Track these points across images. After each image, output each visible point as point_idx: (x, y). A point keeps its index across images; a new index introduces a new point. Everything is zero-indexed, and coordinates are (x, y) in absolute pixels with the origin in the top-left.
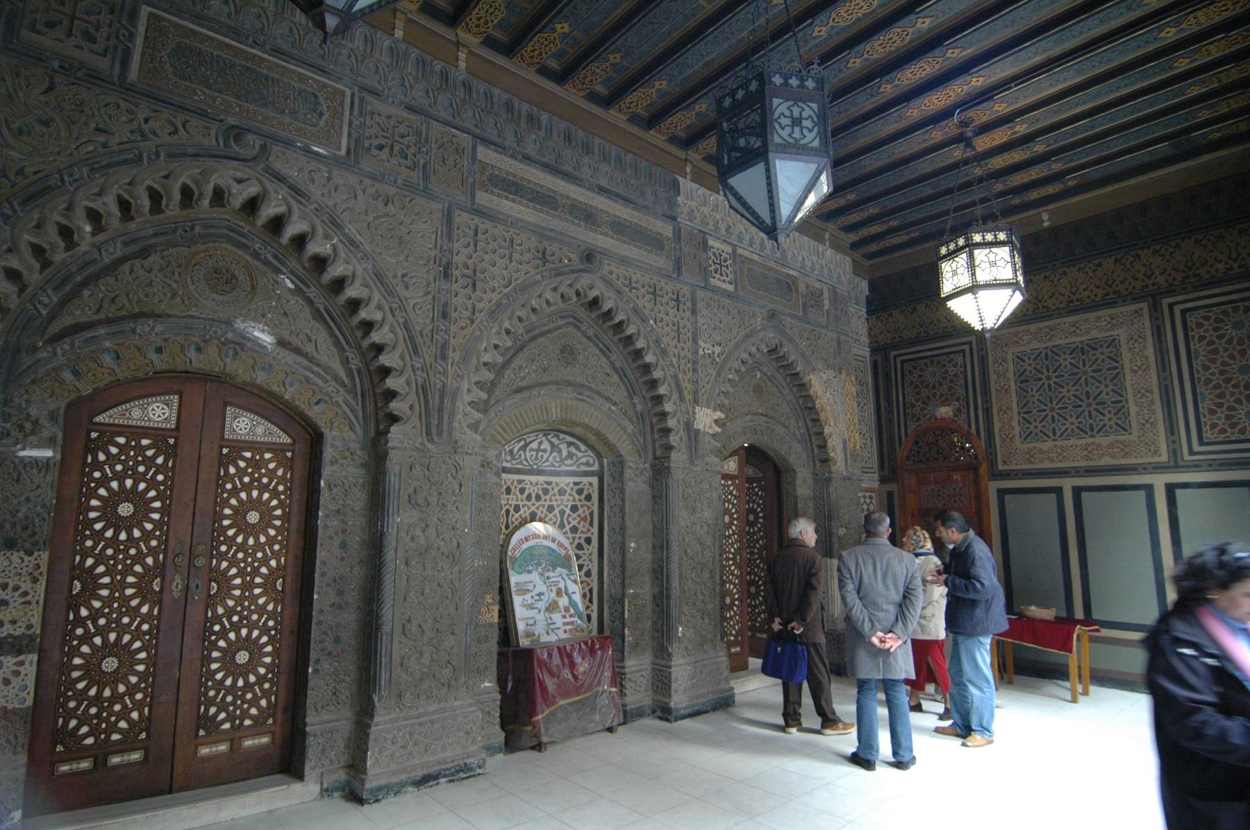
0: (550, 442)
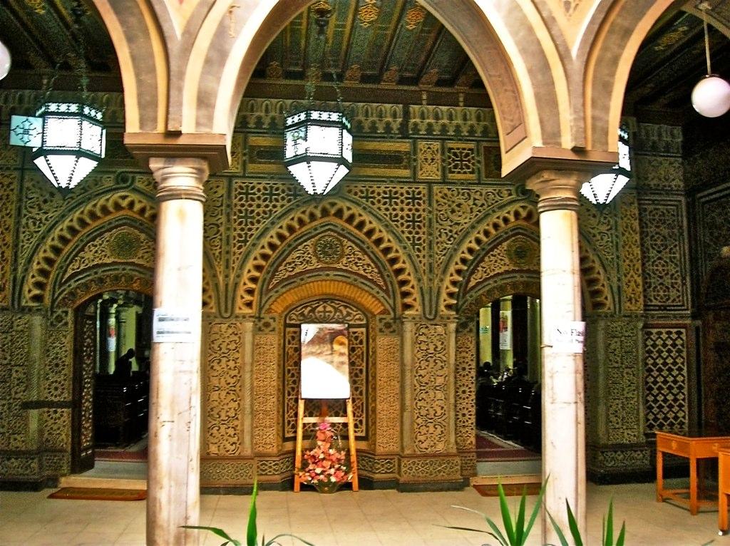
0: (332, 306)
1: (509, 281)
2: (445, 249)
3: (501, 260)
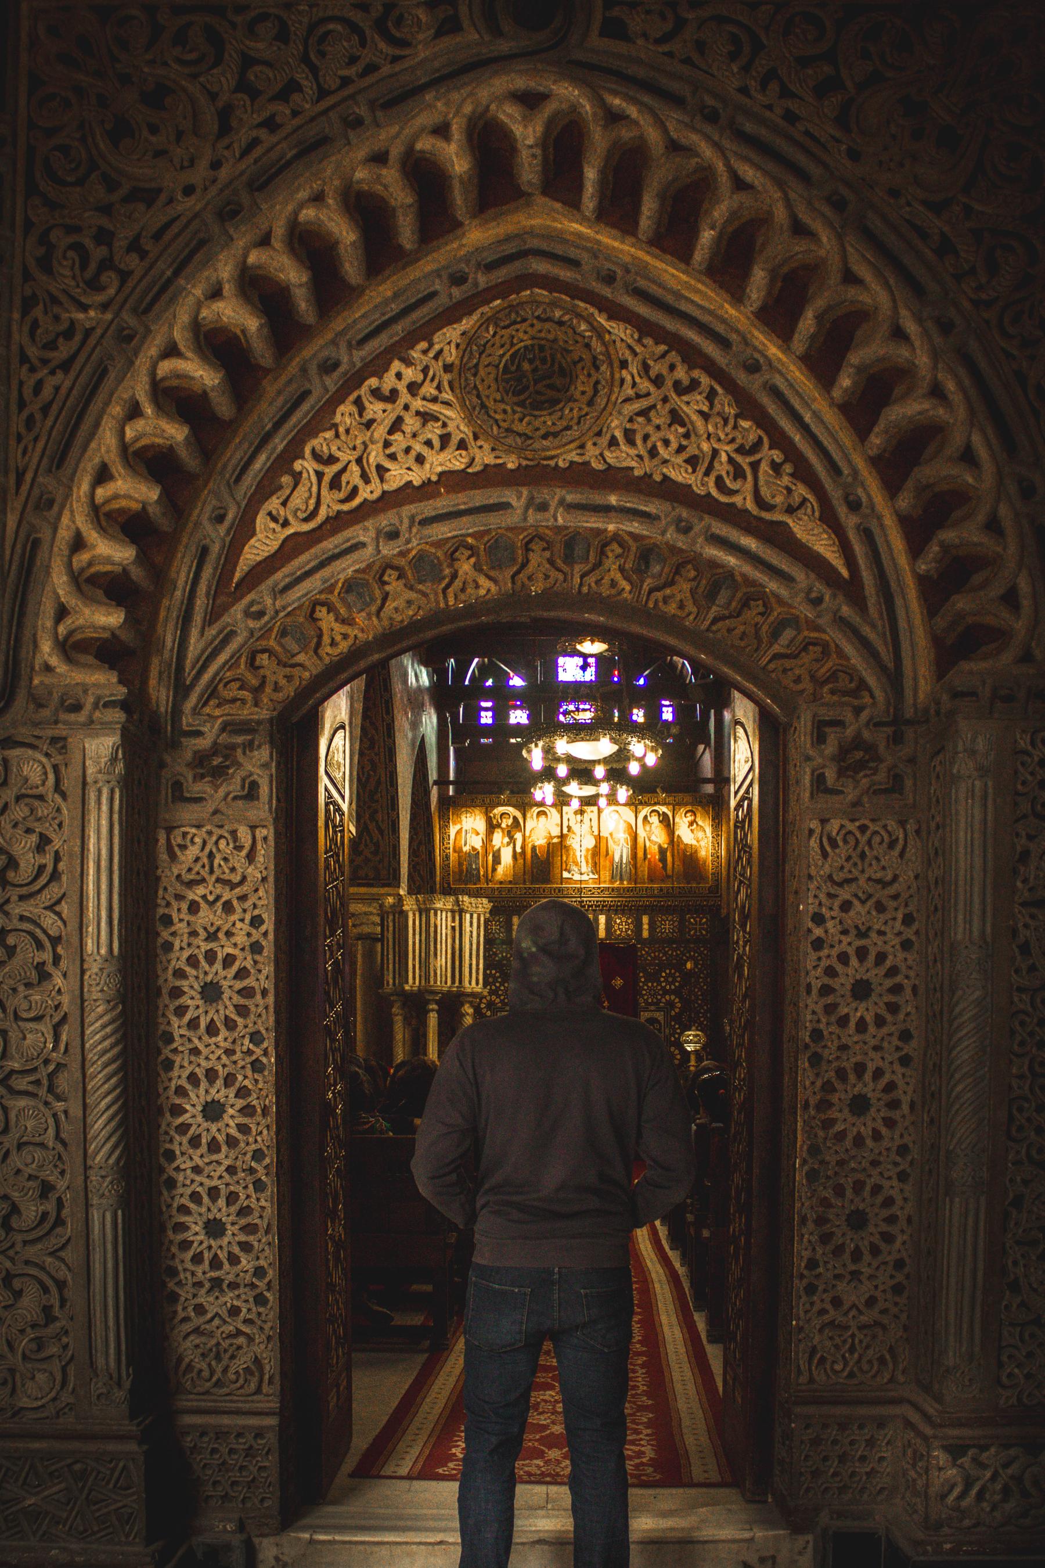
1: (467, 526)
2: (68, 334)
3: (426, 417)
